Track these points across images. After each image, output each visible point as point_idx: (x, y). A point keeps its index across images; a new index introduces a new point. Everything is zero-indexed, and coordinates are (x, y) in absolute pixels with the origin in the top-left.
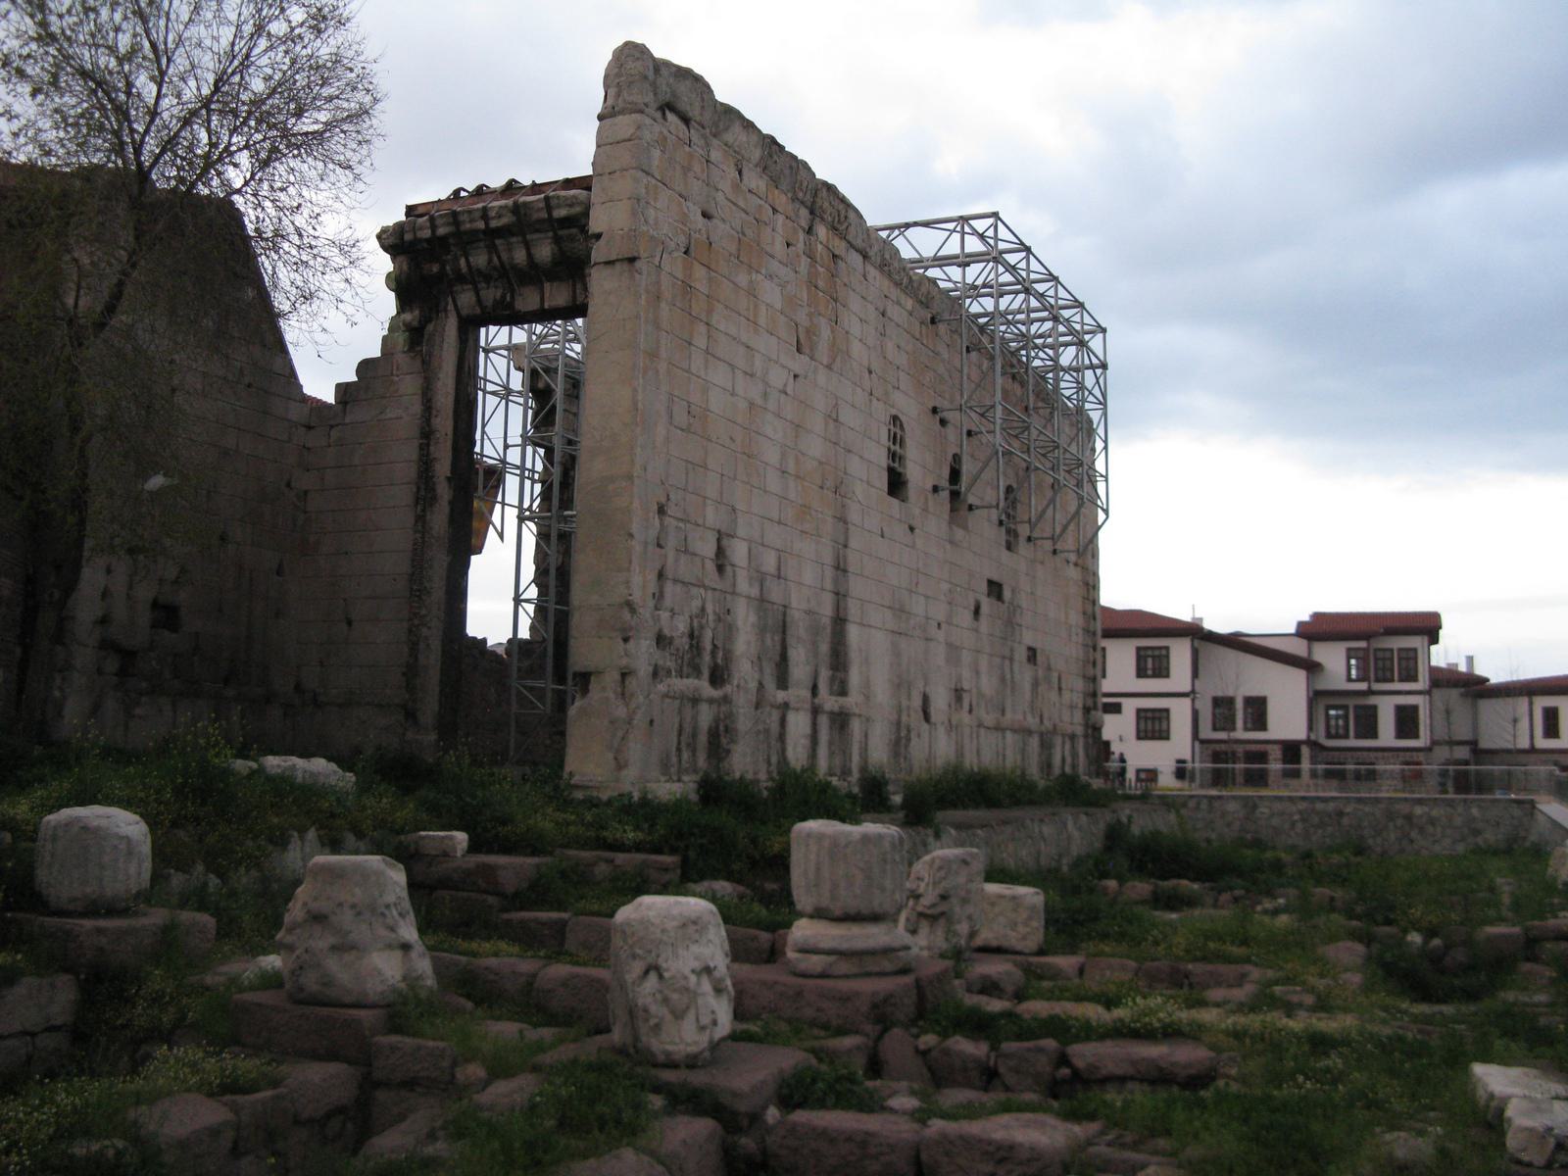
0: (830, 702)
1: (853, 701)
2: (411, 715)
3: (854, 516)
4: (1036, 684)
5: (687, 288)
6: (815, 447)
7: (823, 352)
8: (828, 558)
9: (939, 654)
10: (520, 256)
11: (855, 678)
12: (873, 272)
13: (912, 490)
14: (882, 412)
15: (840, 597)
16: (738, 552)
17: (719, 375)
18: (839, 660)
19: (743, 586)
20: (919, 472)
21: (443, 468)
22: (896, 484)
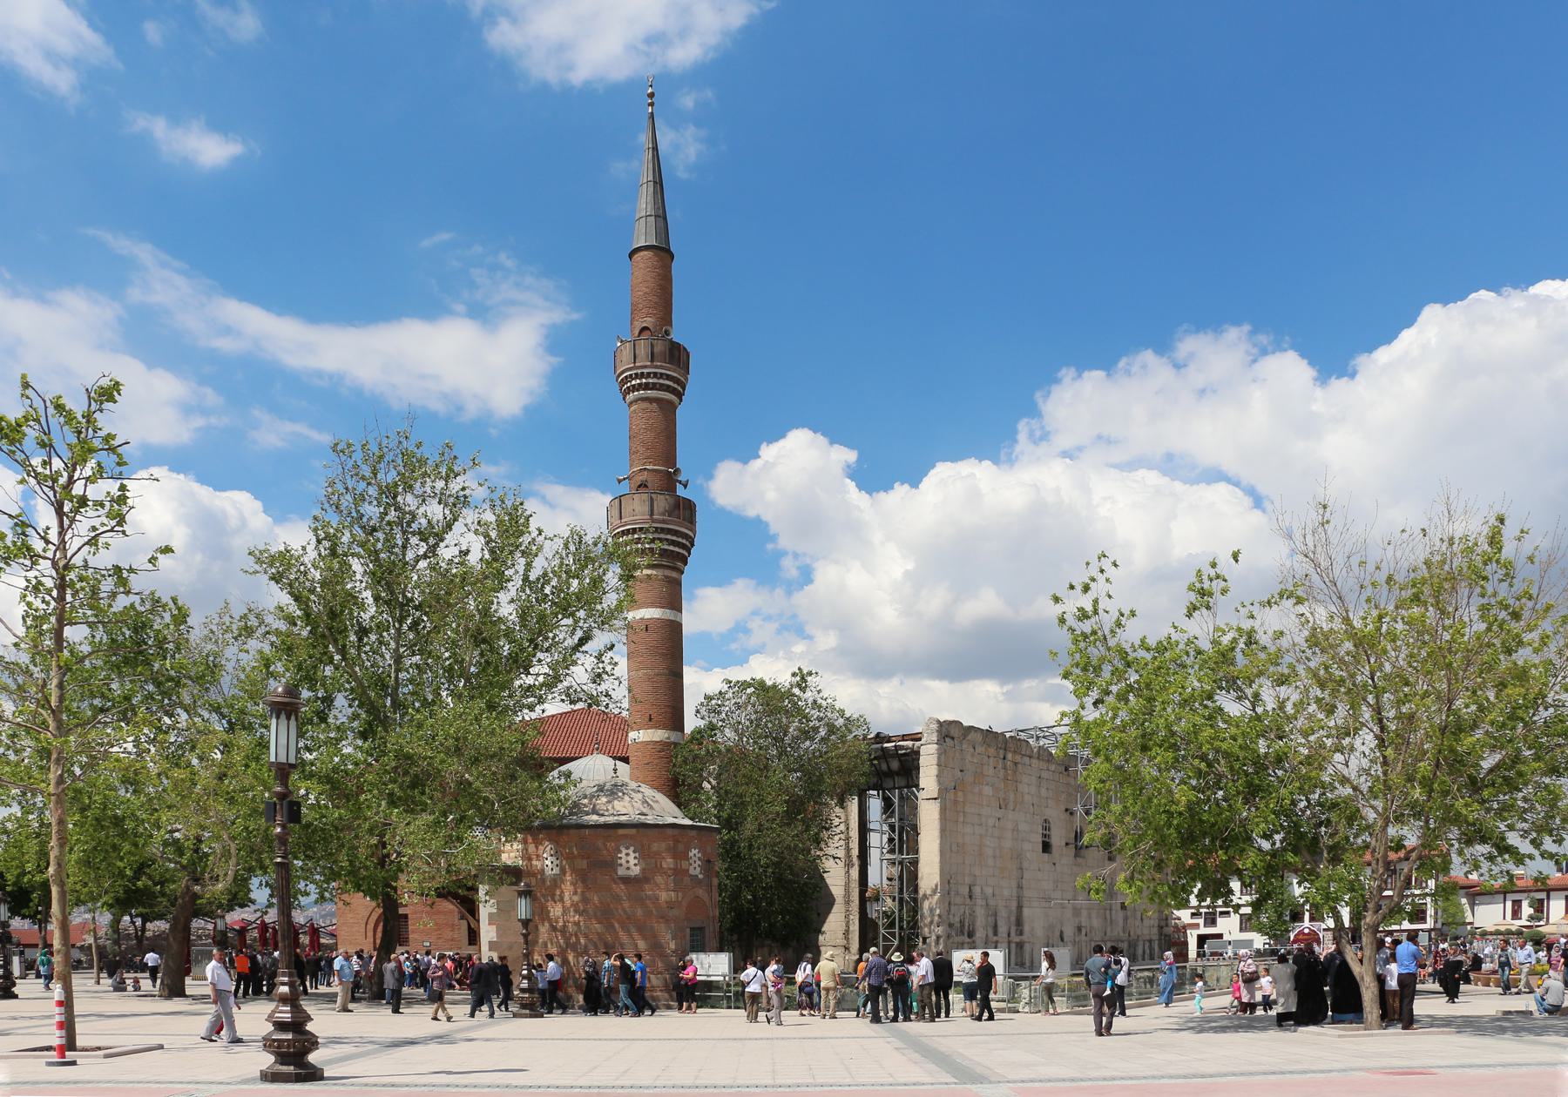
0: (1017, 939)
1: (1024, 938)
2: (847, 948)
3: (1025, 865)
4: (1126, 919)
5: (956, 802)
6: (1008, 844)
7: (1011, 806)
8: (1014, 884)
9: (1069, 913)
10: (884, 767)
11: (1026, 928)
12: (1034, 761)
13: (1054, 850)
14: (1039, 820)
15: (1019, 899)
16: (977, 890)
17: (968, 829)
18: (1019, 922)
19: (979, 902)
20: (1057, 840)
21: (855, 852)
22: (1046, 847)
